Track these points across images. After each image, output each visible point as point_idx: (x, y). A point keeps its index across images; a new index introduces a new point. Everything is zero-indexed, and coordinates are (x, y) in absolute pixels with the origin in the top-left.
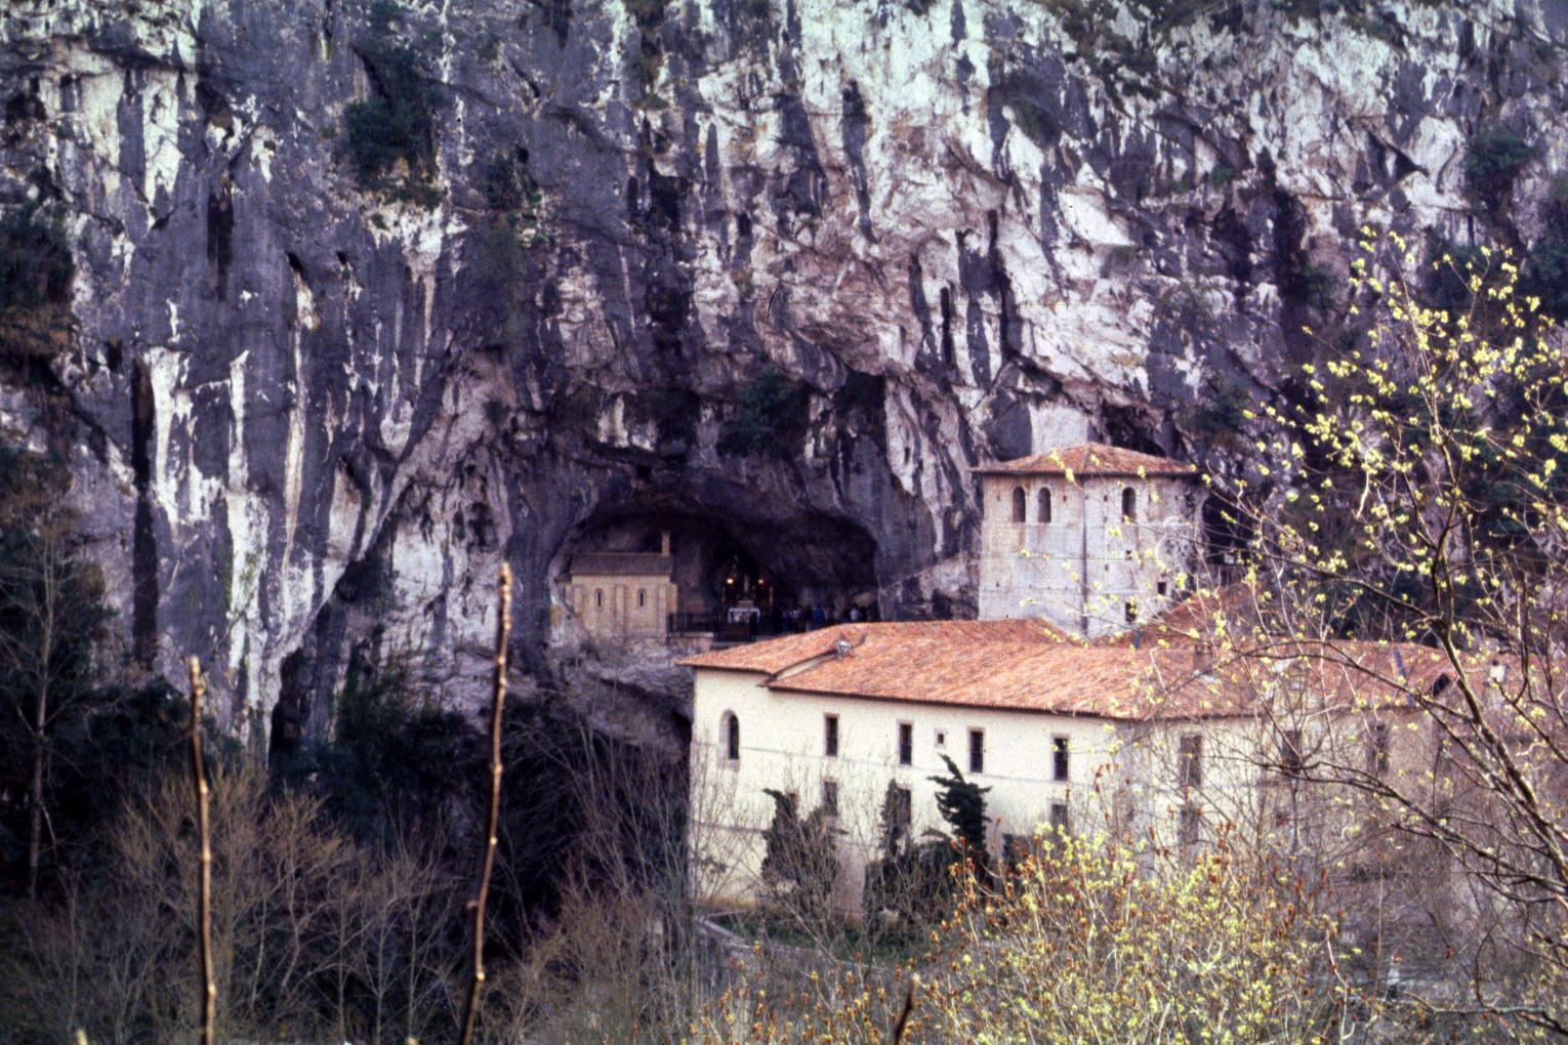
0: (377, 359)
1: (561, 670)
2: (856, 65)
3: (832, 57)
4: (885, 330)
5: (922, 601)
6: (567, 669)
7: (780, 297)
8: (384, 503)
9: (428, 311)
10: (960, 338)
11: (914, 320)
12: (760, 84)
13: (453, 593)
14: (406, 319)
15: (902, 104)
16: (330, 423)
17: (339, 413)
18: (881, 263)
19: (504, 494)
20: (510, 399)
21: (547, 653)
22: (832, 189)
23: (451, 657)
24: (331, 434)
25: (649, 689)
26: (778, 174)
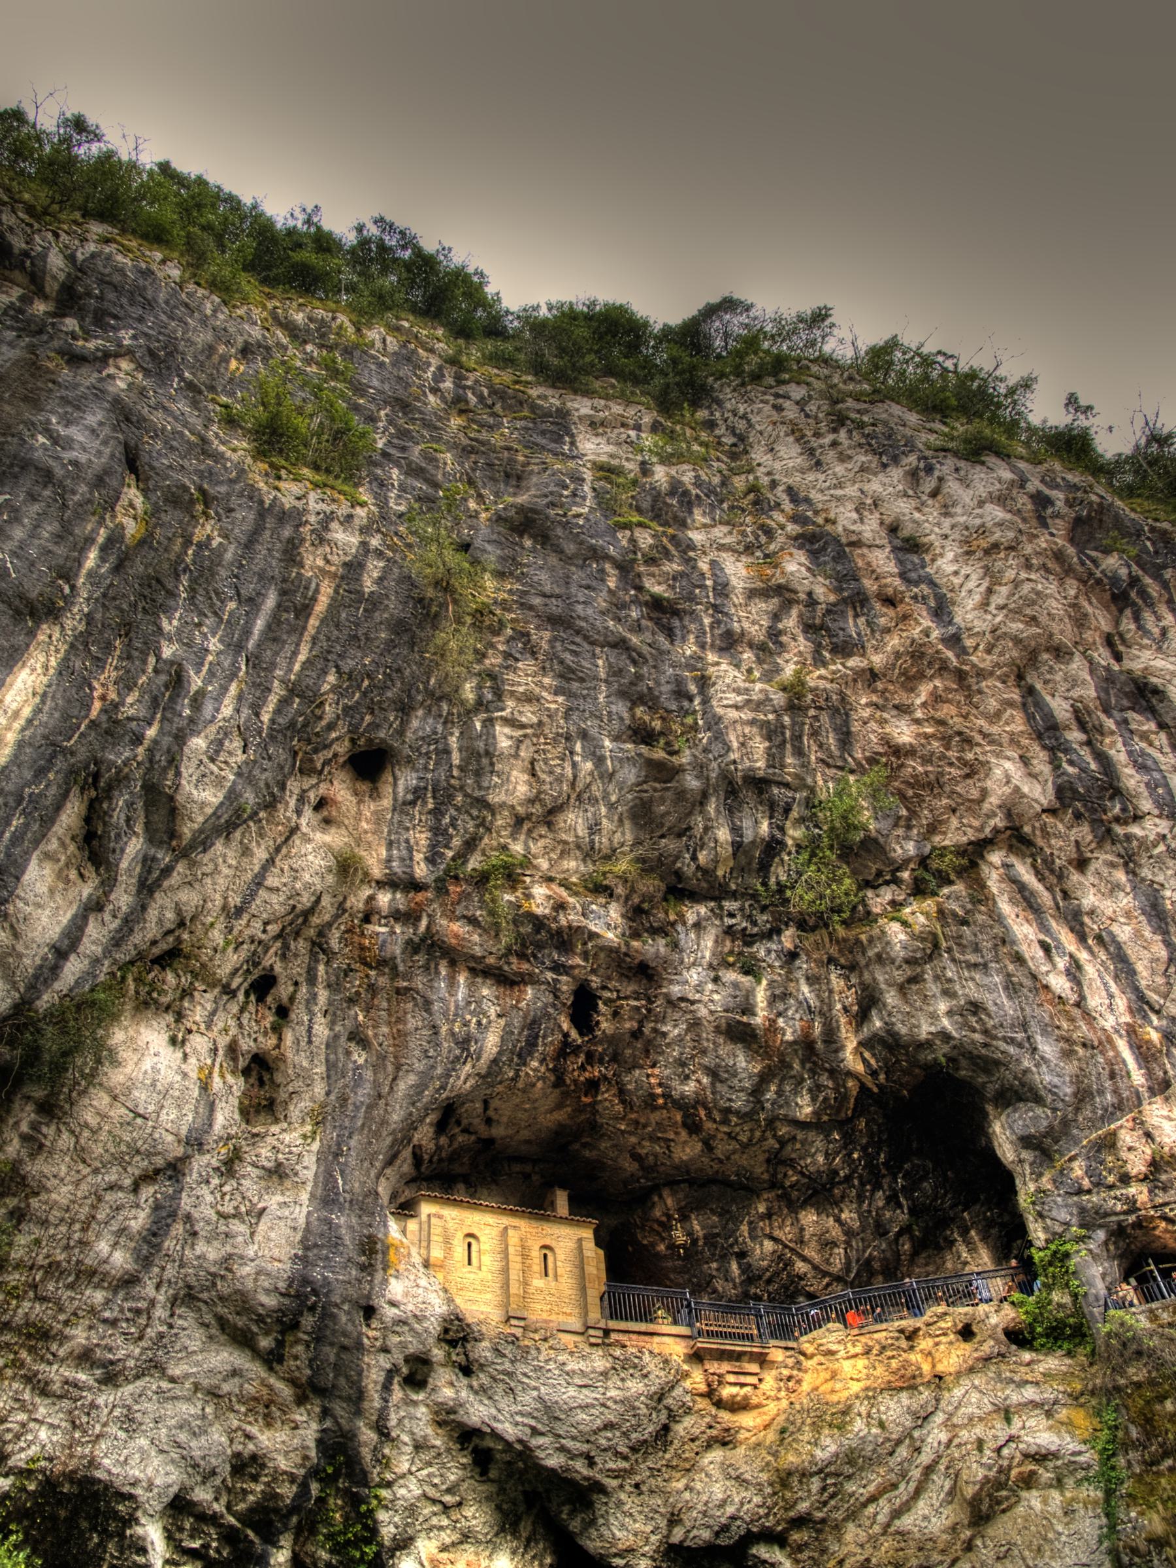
0: (214, 644)
1: (387, 1387)
2: (903, 508)
3: (869, 501)
4: (998, 755)
5: (1125, 1179)
6: (397, 1394)
7: (841, 712)
8: (129, 923)
9: (313, 622)
10: (1119, 754)
11: (1036, 747)
13: (201, 1163)
14: (275, 623)
16: (104, 684)
17: (126, 683)
18: (981, 674)
19: (321, 1030)
20: (374, 861)
21: (371, 1333)
24: (97, 705)
25: (554, 1461)
26: (812, 602)
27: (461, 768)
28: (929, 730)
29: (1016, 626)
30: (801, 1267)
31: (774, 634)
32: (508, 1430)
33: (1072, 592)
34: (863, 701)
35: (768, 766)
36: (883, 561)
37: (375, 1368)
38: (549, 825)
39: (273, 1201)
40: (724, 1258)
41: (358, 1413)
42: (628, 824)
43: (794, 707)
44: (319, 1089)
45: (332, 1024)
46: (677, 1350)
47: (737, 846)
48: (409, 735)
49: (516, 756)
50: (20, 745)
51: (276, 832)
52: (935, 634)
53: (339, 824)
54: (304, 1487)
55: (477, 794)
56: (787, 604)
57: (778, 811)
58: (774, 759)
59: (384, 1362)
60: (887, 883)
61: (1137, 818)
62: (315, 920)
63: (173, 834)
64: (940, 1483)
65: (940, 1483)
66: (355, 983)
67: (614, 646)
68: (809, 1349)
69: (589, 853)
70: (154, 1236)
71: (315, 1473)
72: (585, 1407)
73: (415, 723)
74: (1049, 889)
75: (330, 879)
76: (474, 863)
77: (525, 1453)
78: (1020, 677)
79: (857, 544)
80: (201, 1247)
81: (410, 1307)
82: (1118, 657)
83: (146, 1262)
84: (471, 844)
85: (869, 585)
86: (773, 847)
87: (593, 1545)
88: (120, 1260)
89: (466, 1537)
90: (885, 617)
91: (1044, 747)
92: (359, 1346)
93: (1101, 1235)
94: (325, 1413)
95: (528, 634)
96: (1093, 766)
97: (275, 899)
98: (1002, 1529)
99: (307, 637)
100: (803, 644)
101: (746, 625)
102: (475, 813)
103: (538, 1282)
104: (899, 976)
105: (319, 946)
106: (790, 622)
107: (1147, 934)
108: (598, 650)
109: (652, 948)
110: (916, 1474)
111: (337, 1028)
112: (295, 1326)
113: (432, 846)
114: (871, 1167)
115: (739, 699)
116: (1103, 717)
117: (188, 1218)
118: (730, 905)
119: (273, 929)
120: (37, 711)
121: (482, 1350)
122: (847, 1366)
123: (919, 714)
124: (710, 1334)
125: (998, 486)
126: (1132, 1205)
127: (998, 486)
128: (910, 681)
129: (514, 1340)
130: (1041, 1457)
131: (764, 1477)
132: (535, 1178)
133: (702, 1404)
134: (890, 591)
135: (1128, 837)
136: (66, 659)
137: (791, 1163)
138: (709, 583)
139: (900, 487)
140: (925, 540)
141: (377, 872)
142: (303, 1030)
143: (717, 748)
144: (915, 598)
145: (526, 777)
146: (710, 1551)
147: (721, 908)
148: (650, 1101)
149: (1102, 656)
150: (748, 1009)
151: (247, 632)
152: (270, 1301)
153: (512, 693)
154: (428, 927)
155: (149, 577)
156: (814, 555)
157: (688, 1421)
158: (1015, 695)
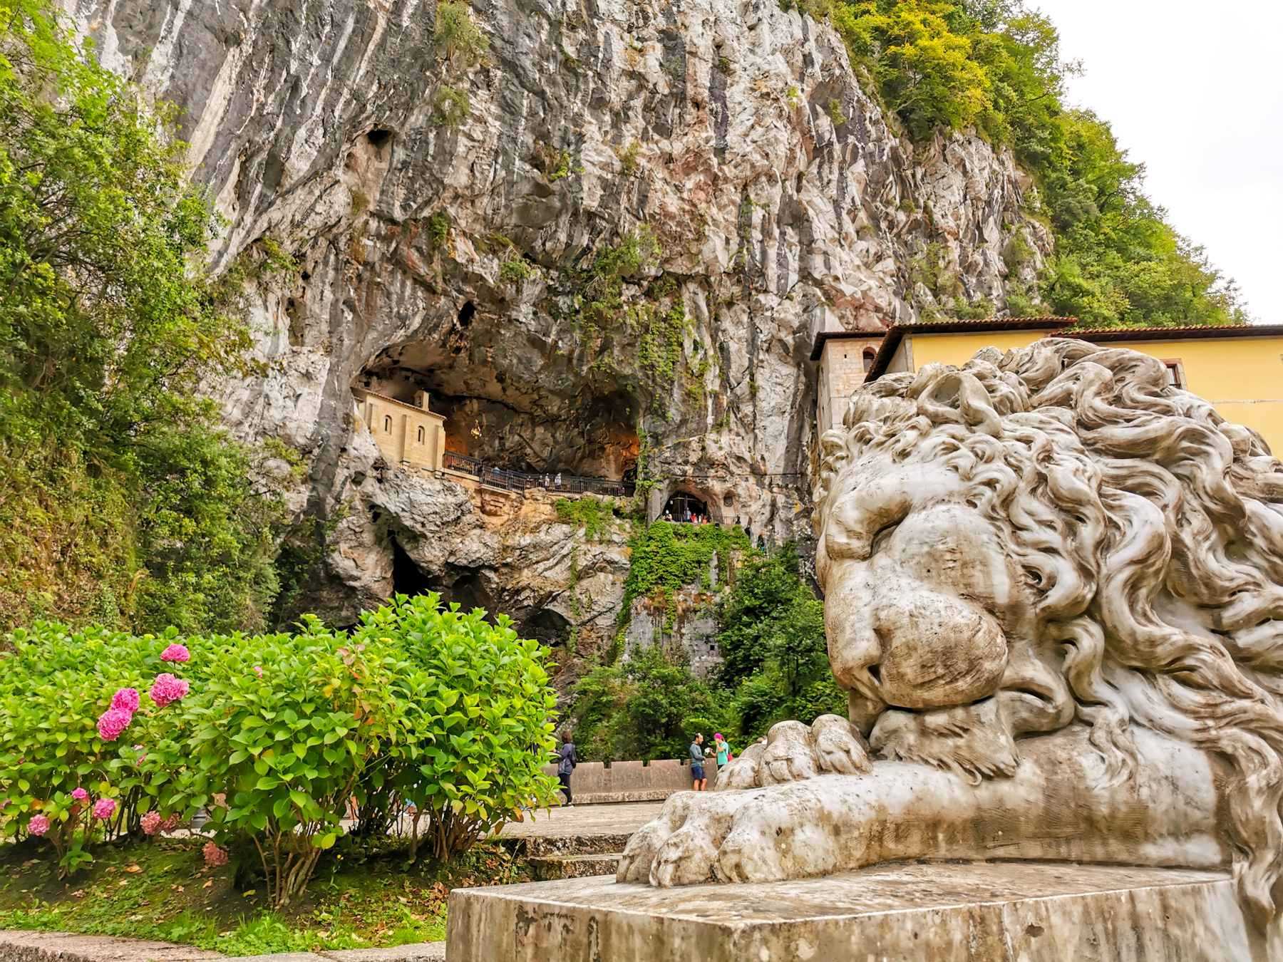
1: (344, 483)
2: (730, 31)
3: (712, 19)
4: (715, 233)
6: (348, 486)
7: (646, 180)
9: (371, 47)
10: (772, 253)
12: (646, 18)
15: (766, 67)
18: (726, 180)
19: (328, 295)
20: (373, 197)
22: (688, 118)
23: (250, 439)
25: (408, 523)
26: (654, 92)
27: (433, 158)
28: (687, 208)
29: (756, 157)
30: (528, 450)
31: (626, 108)
32: (392, 509)
33: (795, 141)
34: (660, 176)
35: (600, 206)
36: (702, 72)
37: (341, 474)
38: (473, 202)
39: (304, 390)
40: (493, 438)
41: (330, 491)
42: (514, 215)
43: (623, 174)
44: (325, 327)
45: (334, 293)
46: (472, 487)
47: (568, 245)
48: (407, 126)
49: (466, 158)
50: (218, 134)
51: (327, 181)
52: (713, 143)
53: (355, 170)
54: (298, 516)
55: (439, 176)
56: (641, 87)
57: (595, 232)
58: (603, 205)
59: (346, 472)
60: (634, 284)
61: (766, 291)
62: (335, 230)
63: (279, 184)
64: (568, 562)
65: (568, 562)
66: (350, 272)
67: (535, 93)
68: (528, 495)
69: (487, 222)
70: (250, 405)
71: (305, 513)
72: (427, 504)
73: (412, 119)
74: (710, 312)
75: (348, 210)
76: (426, 213)
77: (396, 518)
78: (745, 187)
79: (693, 54)
80: (273, 411)
81: (363, 452)
82: (799, 190)
83: (246, 415)
84: (427, 203)
85: (690, 91)
86: (587, 250)
87: (413, 555)
88: (236, 414)
89: (361, 544)
90: (691, 114)
91: (739, 235)
92: (336, 465)
93: (667, 482)
94: (314, 489)
95: (488, 71)
96: (758, 258)
97: (318, 218)
98: (585, 583)
99: (366, 58)
100: (641, 123)
101: (613, 96)
102: (435, 186)
103: (416, 444)
104: (626, 341)
105: (333, 242)
106: (638, 103)
107: (744, 352)
108: (526, 93)
109: (510, 290)
110: (558, 557)
111: (338, 295)
112: (310, 452)
113: (406, 199)
114: (577, 419)
115: (596, 159)
116: (775, 226)
117: (267, 396)
118: (554, 273)
119: (313, 233)
120: (226, 112)
121: (390, 474)
122: (542, 507)
123: (685, 195)
124: (489, 483)
125: (789, 41)
126: (684, 473)
127: (789, 41)
128: (689, 169)
129: (403, 472)
130: (610, 562)
131: (496, 546)
132: (412, 379)
133: (478, 511)
134: (700, 98)
135: (758, 301)
136: (240, 73)
137: (542, 407)
138: (601, 56)
139: (734, 15)
140: (732, 66)
141: (371, 207)
142: (318, 291)
143: (575, 186)
144: (711, 110)
145: (467, 171)
146: (465, 568)
147: (548, 273)
148: (484, 362)
149: (791, 186)
150: (547, 334)
151: (334, 51)
152: (302, 441)
153: (472, 114)
154: (396, 249)
155: (287, 9)
156: (668, 50)
157: (468, 516)
158: (737, 198)
